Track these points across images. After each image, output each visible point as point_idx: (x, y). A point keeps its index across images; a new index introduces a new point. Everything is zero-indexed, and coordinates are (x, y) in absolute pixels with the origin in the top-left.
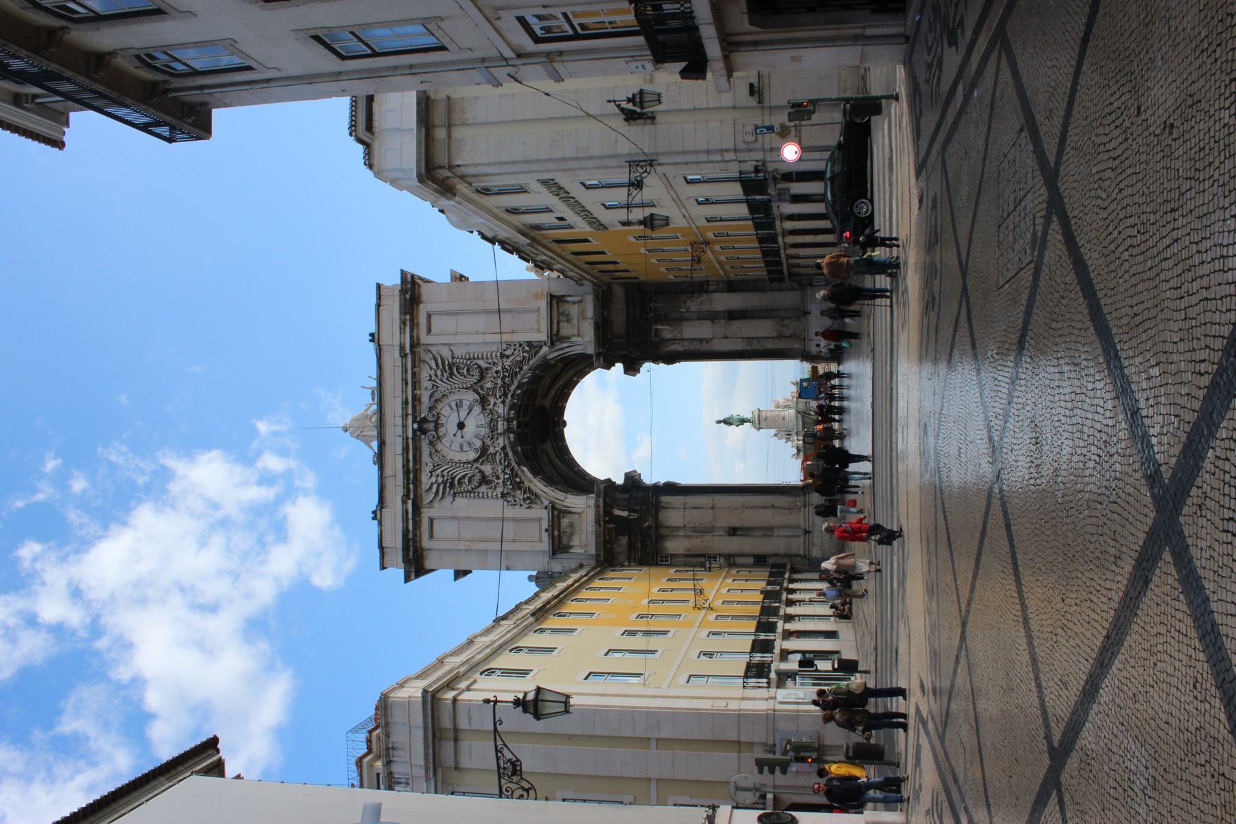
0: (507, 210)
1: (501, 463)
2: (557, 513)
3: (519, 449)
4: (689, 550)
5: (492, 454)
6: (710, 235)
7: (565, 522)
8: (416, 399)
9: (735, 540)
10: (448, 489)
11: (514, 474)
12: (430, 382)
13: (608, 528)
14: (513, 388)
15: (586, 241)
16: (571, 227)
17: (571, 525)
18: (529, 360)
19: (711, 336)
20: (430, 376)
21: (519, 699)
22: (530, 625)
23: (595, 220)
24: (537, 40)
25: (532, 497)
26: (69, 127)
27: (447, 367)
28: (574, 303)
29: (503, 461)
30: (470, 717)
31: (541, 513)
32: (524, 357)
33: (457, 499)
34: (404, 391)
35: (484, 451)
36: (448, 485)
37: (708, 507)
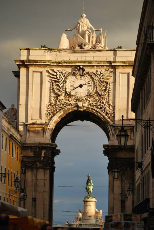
1: (65, 103)
4: (27, 182)
5: (68, 99)
9: (31, 201)
10: (54, 80)
13: (37, 148)
14: (96, 109)
18: (107, 116)
19: (114, 193)
29: (65, 104)
31: (44, 120)
32: (109, 114)
33: (50, 83)
34: (96, 62)
36: (56, 80)
37: (45, 190)
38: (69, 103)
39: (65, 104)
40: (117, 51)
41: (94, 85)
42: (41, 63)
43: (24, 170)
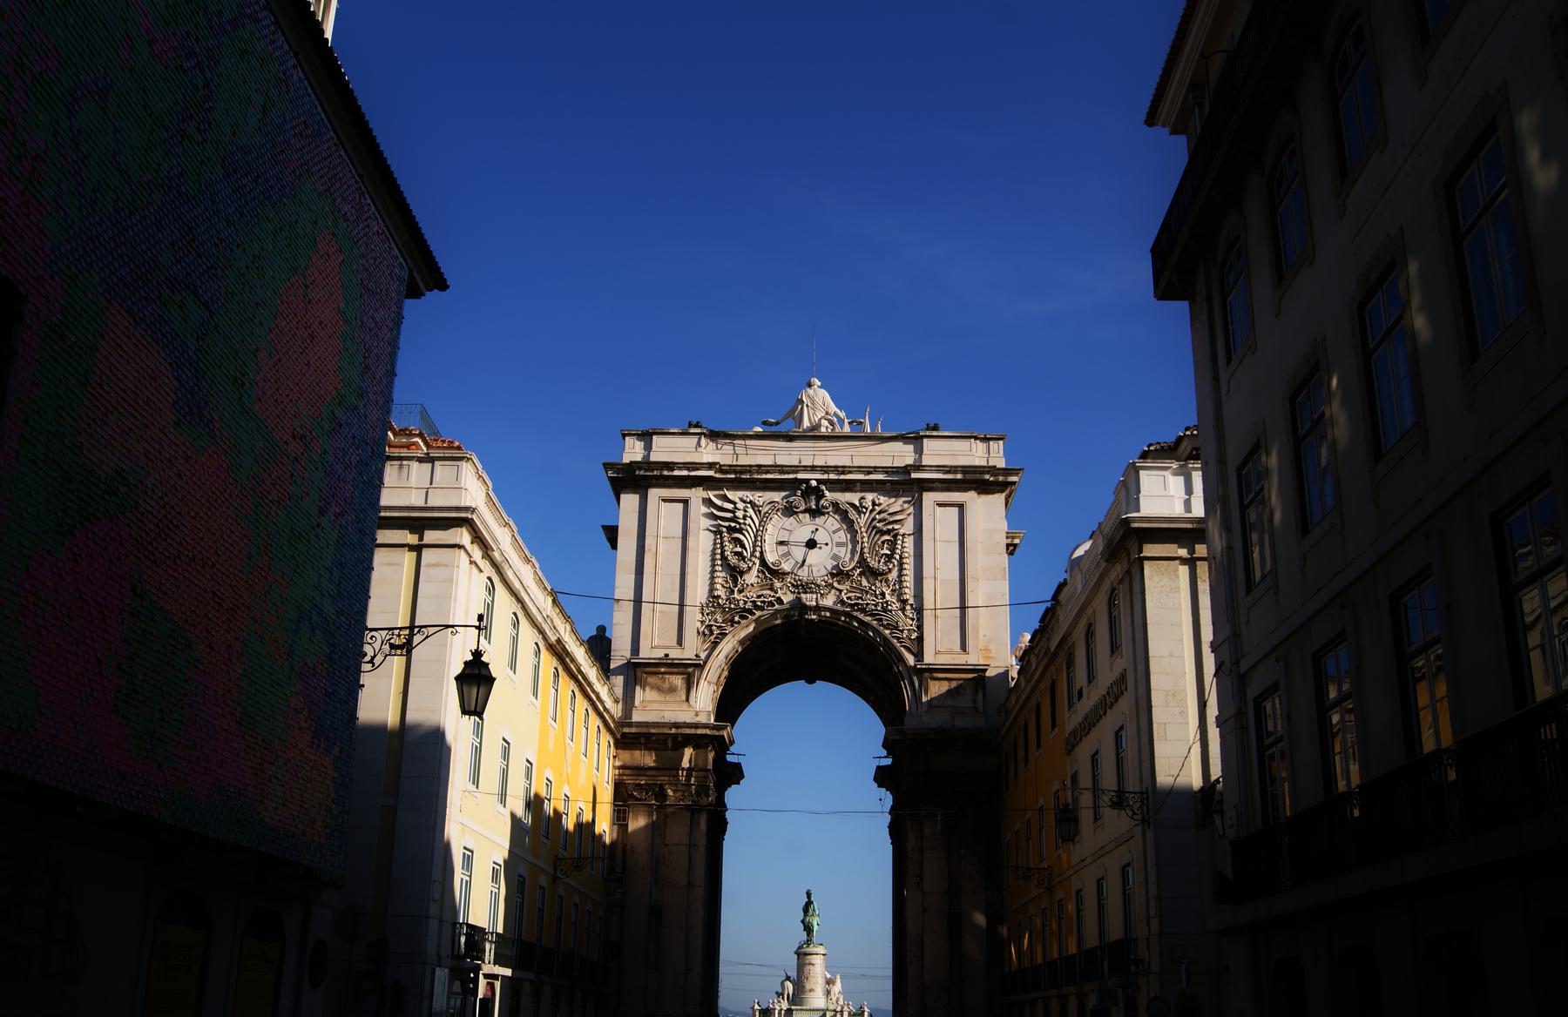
0: (1090, 625)
1: (759, 597)
2: (690, 671)
3: (779, 622)
5: (772, 584)
6: (1060, 895)
7: (678, 681)
8: (848, 486)
10: (727, 524)
11: (745, 613)
12: (870, 504)
13: (667, 739)
15: (1054, 727)
16: (1070, 707)
17: (672, 690)
18: (898, 638)
20: (879, 505)
21: (482, 655)
22: (545, 638)
23: (1078, 739)
24: (1259, 702)
25: (712, 638)
26: (1171, 134)
27: (890, 527)
28: (974, 701)
29: (762, 599)
30: (437, 565)
31: (692, 648)
32: (902, 631)
34: (860, 469)
35: (777, 573)
36: (733, 524)
38: (773, 596)
39: (762, 599)
40: (925, 440)
41: (854, 542)
42: (685, 473)
43: (625, 811)
